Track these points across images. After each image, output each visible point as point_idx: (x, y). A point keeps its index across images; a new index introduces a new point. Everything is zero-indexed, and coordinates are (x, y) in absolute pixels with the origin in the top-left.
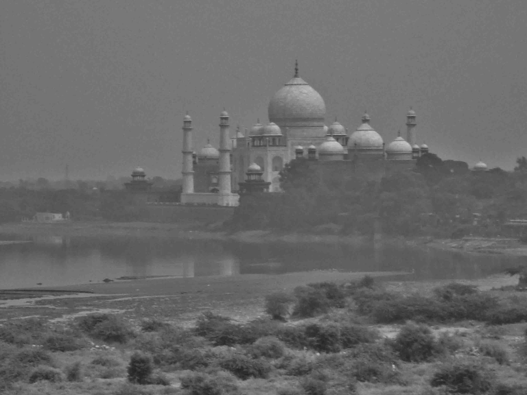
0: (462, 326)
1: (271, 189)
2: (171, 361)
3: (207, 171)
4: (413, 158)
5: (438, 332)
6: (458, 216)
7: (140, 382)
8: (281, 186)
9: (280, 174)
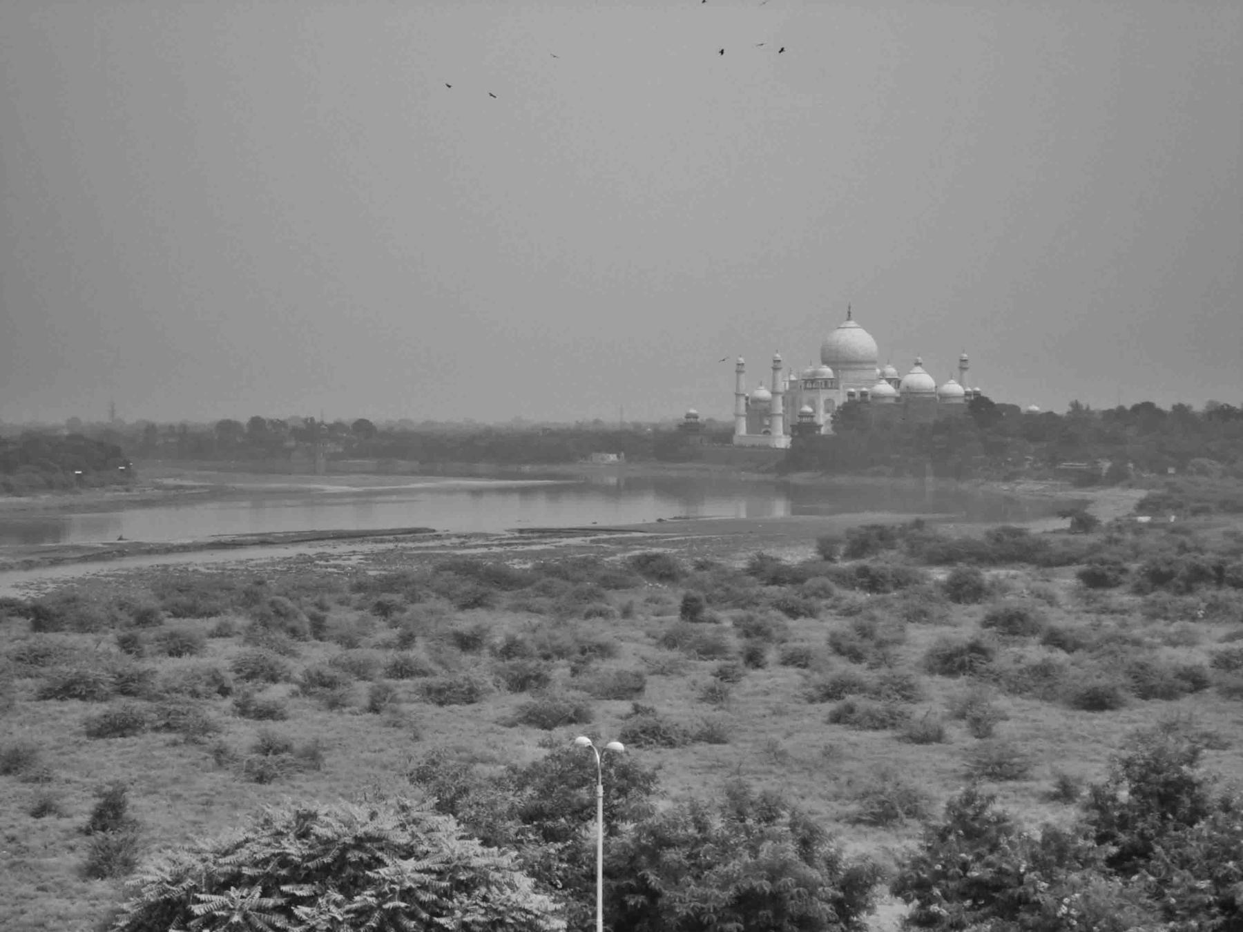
1: (823, 431)
2: (722, 600)
3: (759, 413)
5: (989, 574)
8: (834, 429)
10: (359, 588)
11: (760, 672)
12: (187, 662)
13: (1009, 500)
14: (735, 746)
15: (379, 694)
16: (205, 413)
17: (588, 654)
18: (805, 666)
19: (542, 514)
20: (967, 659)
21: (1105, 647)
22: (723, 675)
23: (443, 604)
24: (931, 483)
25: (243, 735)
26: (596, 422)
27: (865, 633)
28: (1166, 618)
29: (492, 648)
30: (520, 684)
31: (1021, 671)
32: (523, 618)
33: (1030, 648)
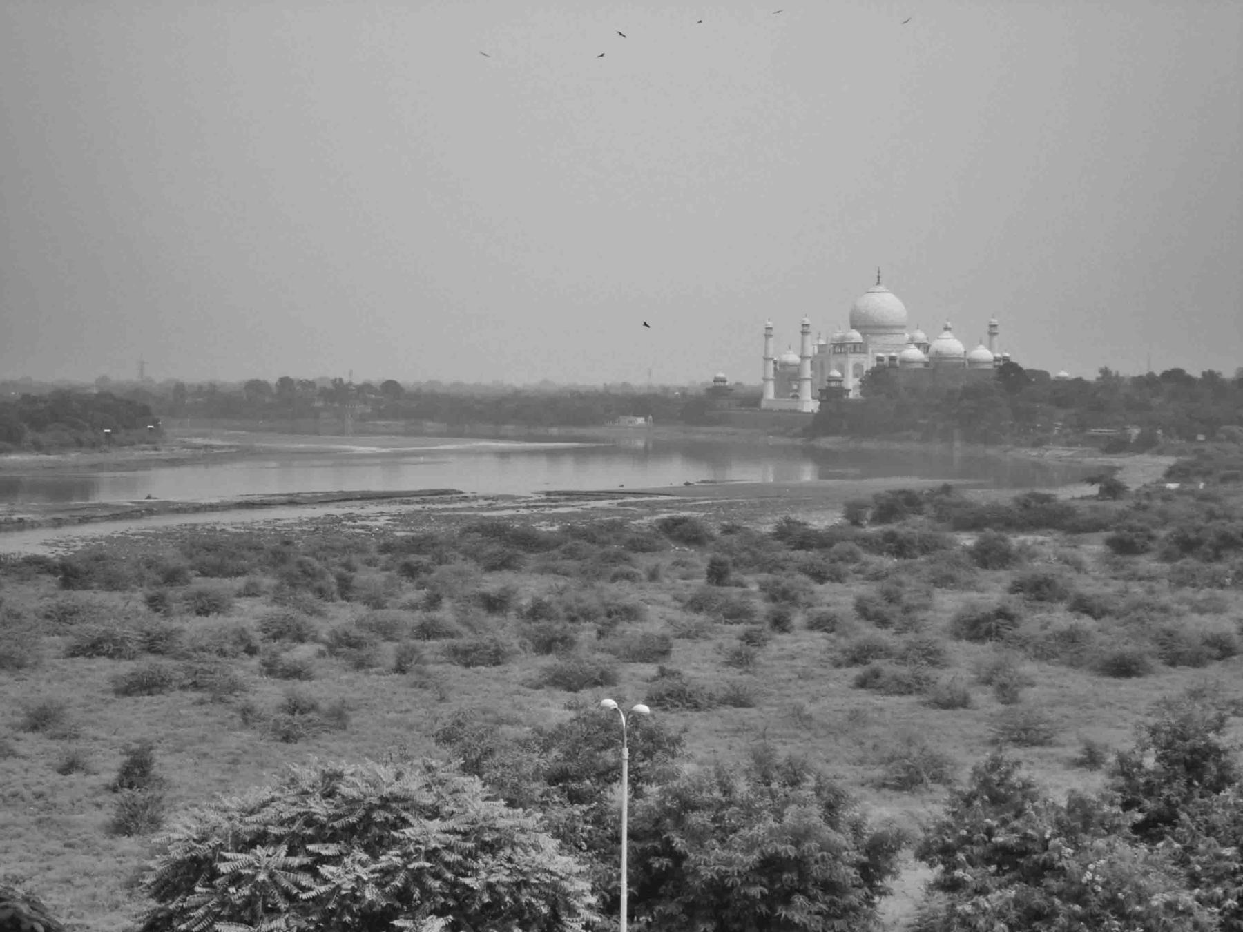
1: (851, 395)
2: (748, 564)
3: (787, 377)
5: (1016, 540)
7: (718, 584)
8: (861, 393)
10: (386, 549)
11: (785, 637)
12: (213, 621)
13: (1037, 466)
14: (761, 709)
15: (404, 655)
16: (231, 370)
17: (615, 616)
18: (832, 631)
19: (569, 476)
20: (994, 624)
21: (1132, 614)
22: (749, 639)
23: (469, 566)
24: (959, 449)
25: (269, 694)
26: (625, 385)
27: (891, 598)
28: (1194, 586)
29: (519, 610)
30: (546, 646)
31: (1047, 638)
32: (549, 581)
33: (1058, 614)
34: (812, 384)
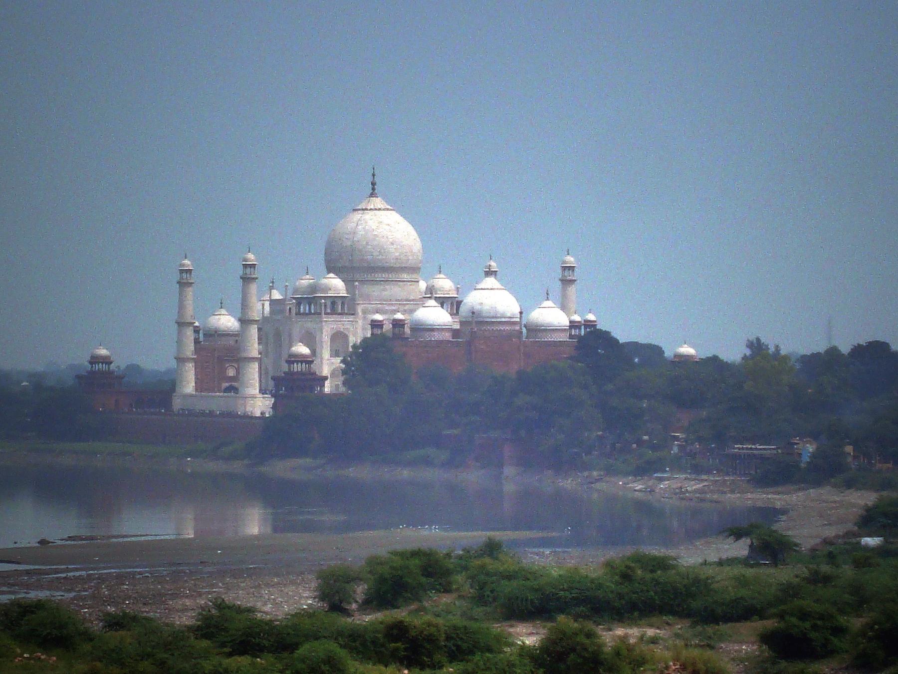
0: (651, 626)
1: (327, 390)
3: (218, 356)
4: (571, 336)
5: (612, 636)
6: (646, 438)
8: (344, 383)
9: (343, 362)
13: (643, 507)
24: (512, 479)
34: (260, 368)
